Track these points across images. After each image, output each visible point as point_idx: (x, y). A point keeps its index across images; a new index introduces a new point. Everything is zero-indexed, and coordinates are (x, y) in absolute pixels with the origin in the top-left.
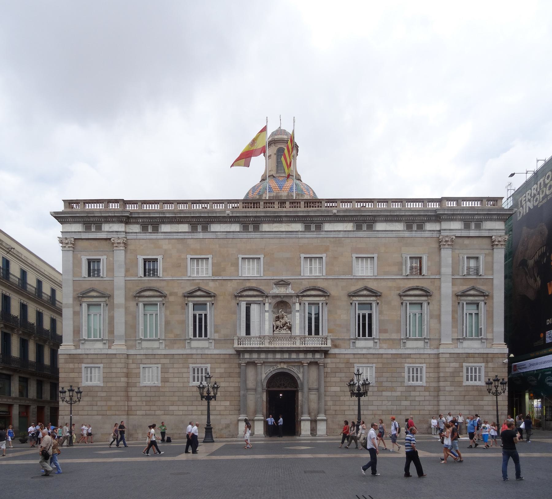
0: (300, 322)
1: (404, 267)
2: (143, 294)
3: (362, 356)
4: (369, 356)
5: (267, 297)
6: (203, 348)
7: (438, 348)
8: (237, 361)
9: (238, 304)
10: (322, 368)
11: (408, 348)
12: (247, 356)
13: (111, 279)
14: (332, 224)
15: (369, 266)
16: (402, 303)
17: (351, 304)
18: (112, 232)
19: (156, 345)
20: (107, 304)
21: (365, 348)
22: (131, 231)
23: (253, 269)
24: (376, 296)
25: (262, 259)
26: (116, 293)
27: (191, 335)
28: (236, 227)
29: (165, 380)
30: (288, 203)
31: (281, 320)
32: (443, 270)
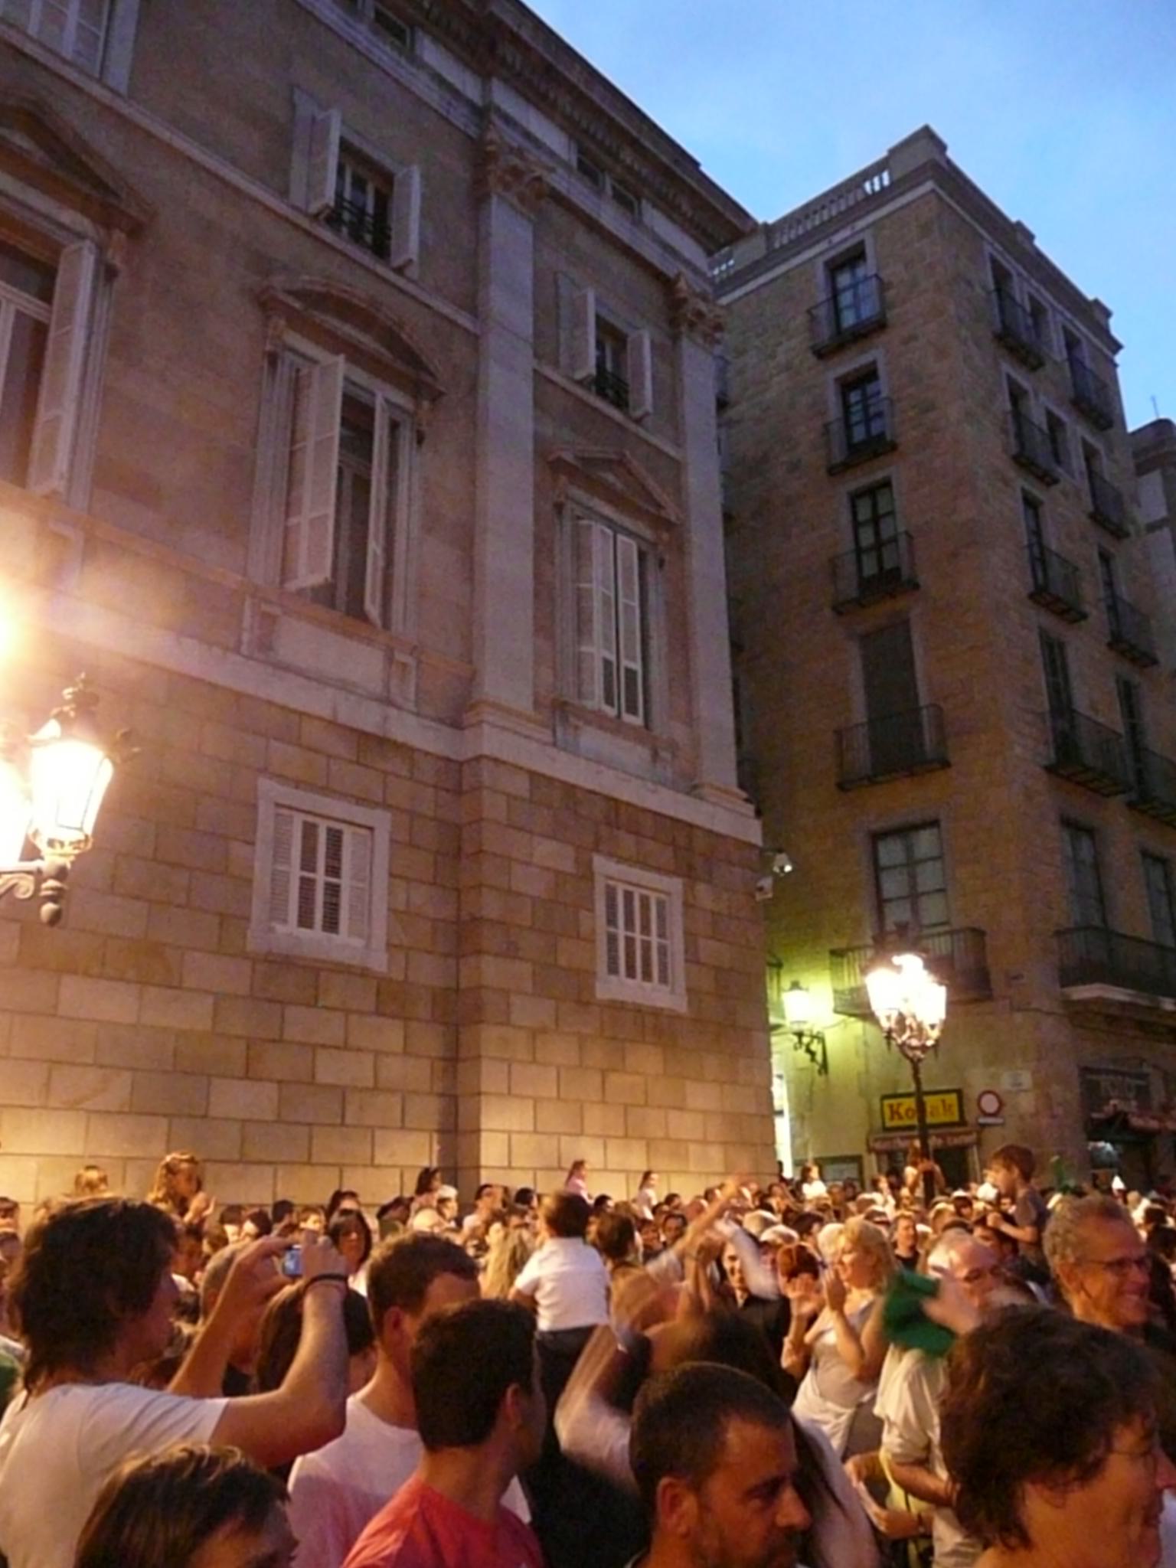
11: (287, 668)
16: (273, 359)
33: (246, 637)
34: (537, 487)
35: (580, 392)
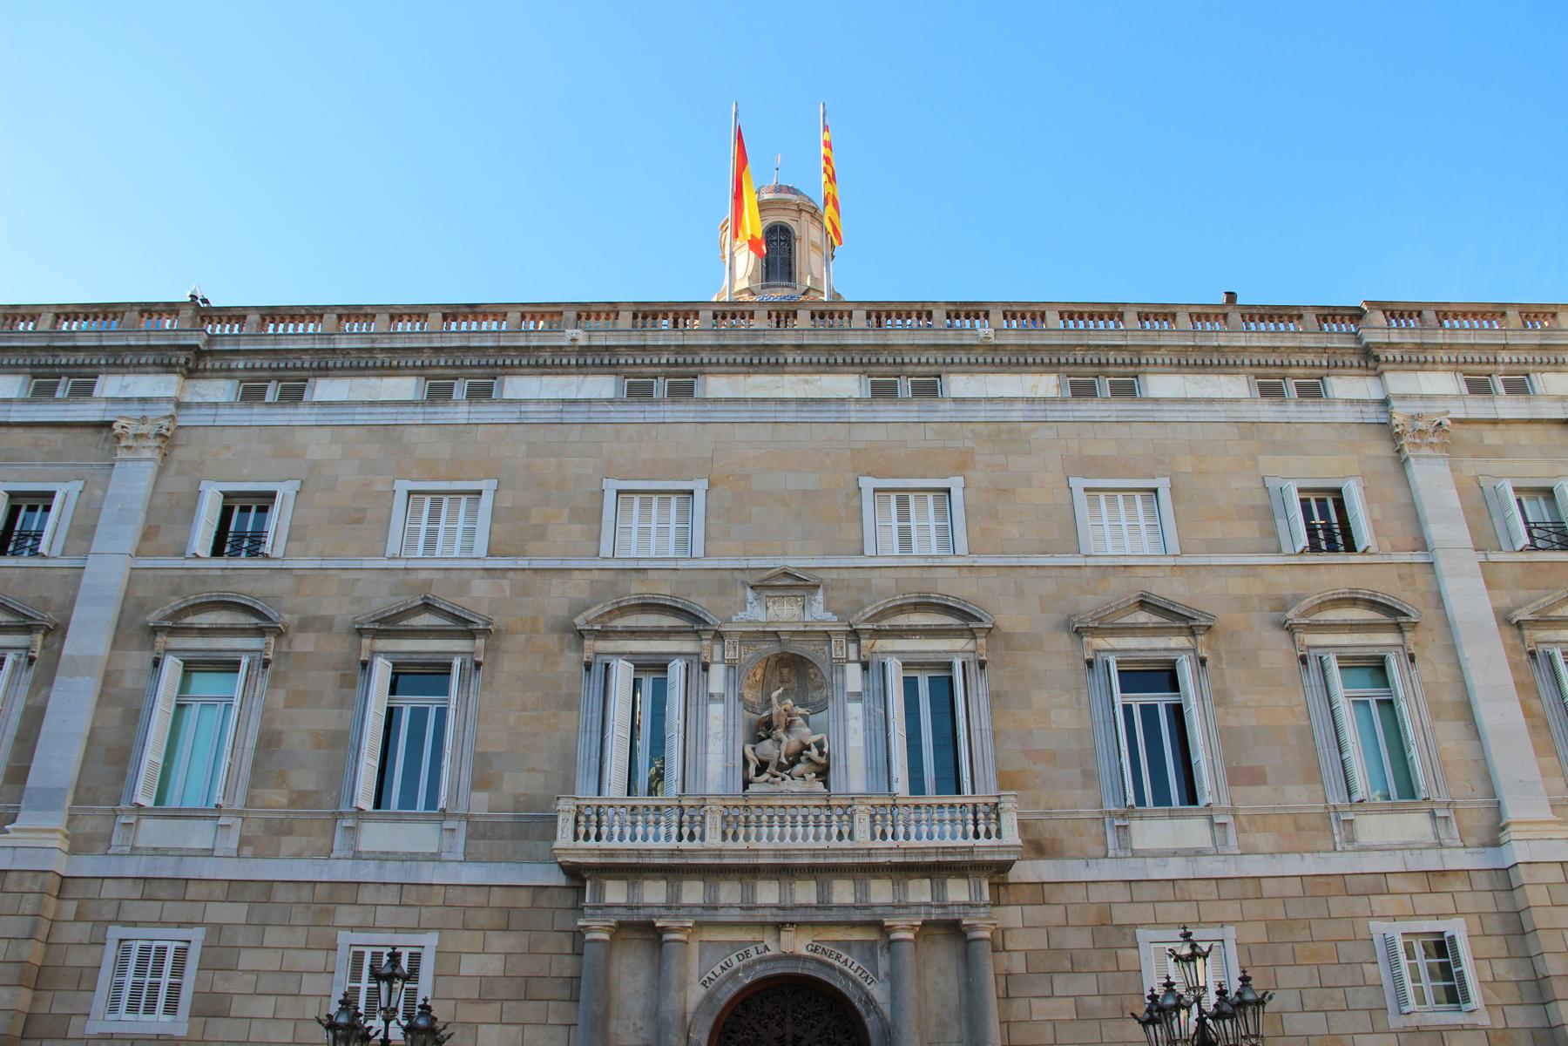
0: (869, 743)
1: (1281, 524)
2: (190, 620)
3: (1168, 892)
4: (1197, 890)
5: (719, 636)
6: (413, 857)
7: (1496, 844)
8: (564, 920)
9: (588, 666)
11: (1366, 849)
12: (615, 892)
13: (78, 563)
14: (982, 376)
15: (1142, 522)
16: (1303, 660)
17: (1090, 663)
18: (127, 400)
19: (199, 835)
20: (31, 660)
21: (1175, 853)
22: (199, 399)
24: (1192, 632)
25: (700, 496)
26: (80, 614)
27: (365, 800)
28: (602, 386)
29: (210, 1007)
30: (803, 320)
32: (1436, 532)
33: (1337, 839)
34: (1510, 649)
35: (1524, 557)
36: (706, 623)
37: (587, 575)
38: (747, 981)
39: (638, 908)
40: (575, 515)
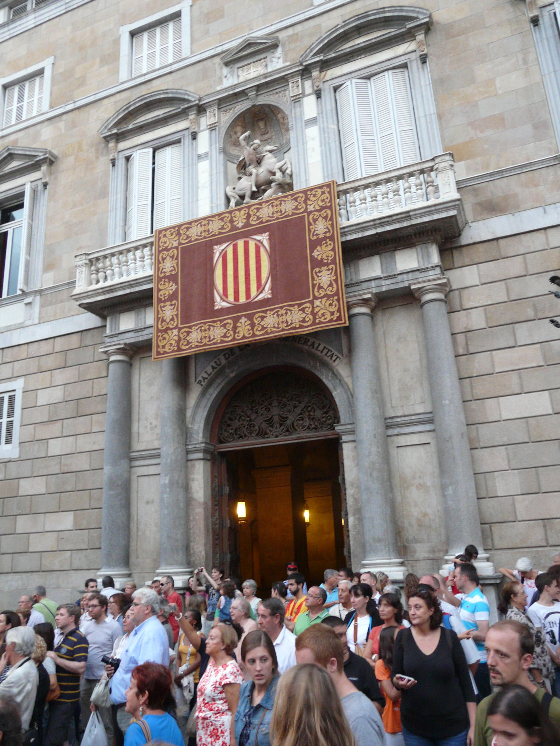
5: (201, 109)
10: (434, 312)
12: (127, 322)
23: (164, 50)
31: (252, 169)
36: (188, 101)
37: (112, 99)
38: (232, 375)
39: (142, 330)
40: (104, 61)
